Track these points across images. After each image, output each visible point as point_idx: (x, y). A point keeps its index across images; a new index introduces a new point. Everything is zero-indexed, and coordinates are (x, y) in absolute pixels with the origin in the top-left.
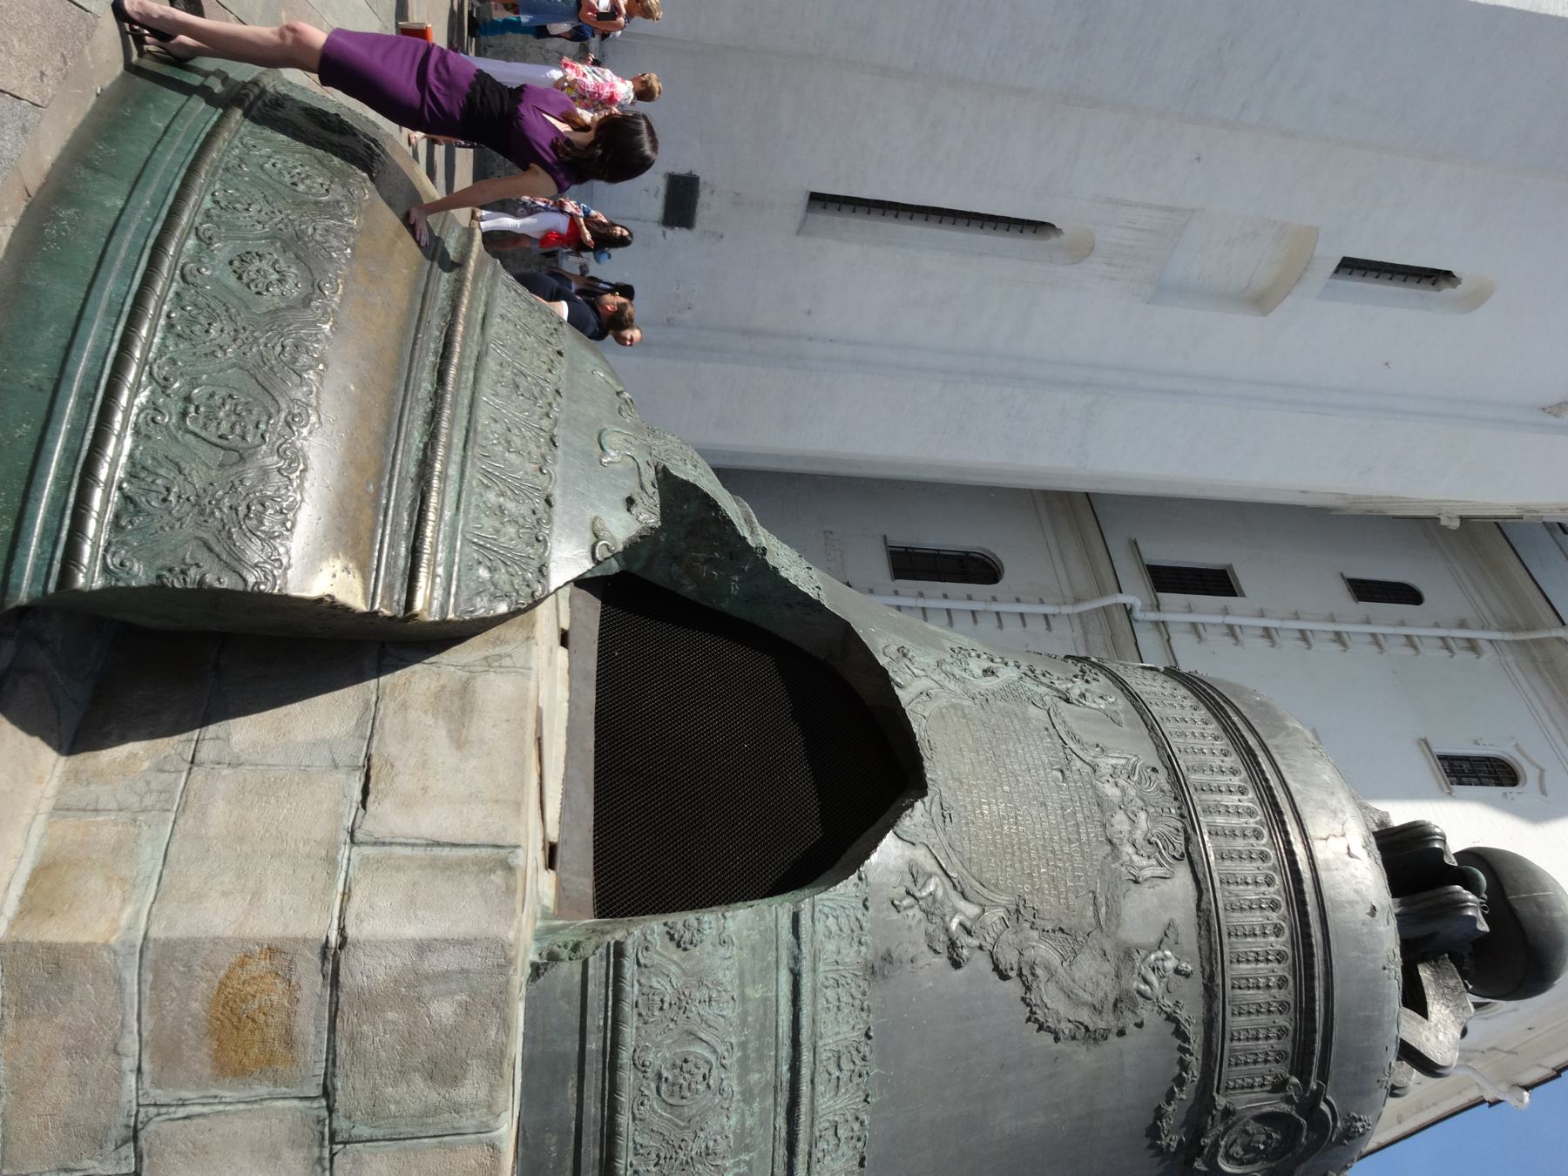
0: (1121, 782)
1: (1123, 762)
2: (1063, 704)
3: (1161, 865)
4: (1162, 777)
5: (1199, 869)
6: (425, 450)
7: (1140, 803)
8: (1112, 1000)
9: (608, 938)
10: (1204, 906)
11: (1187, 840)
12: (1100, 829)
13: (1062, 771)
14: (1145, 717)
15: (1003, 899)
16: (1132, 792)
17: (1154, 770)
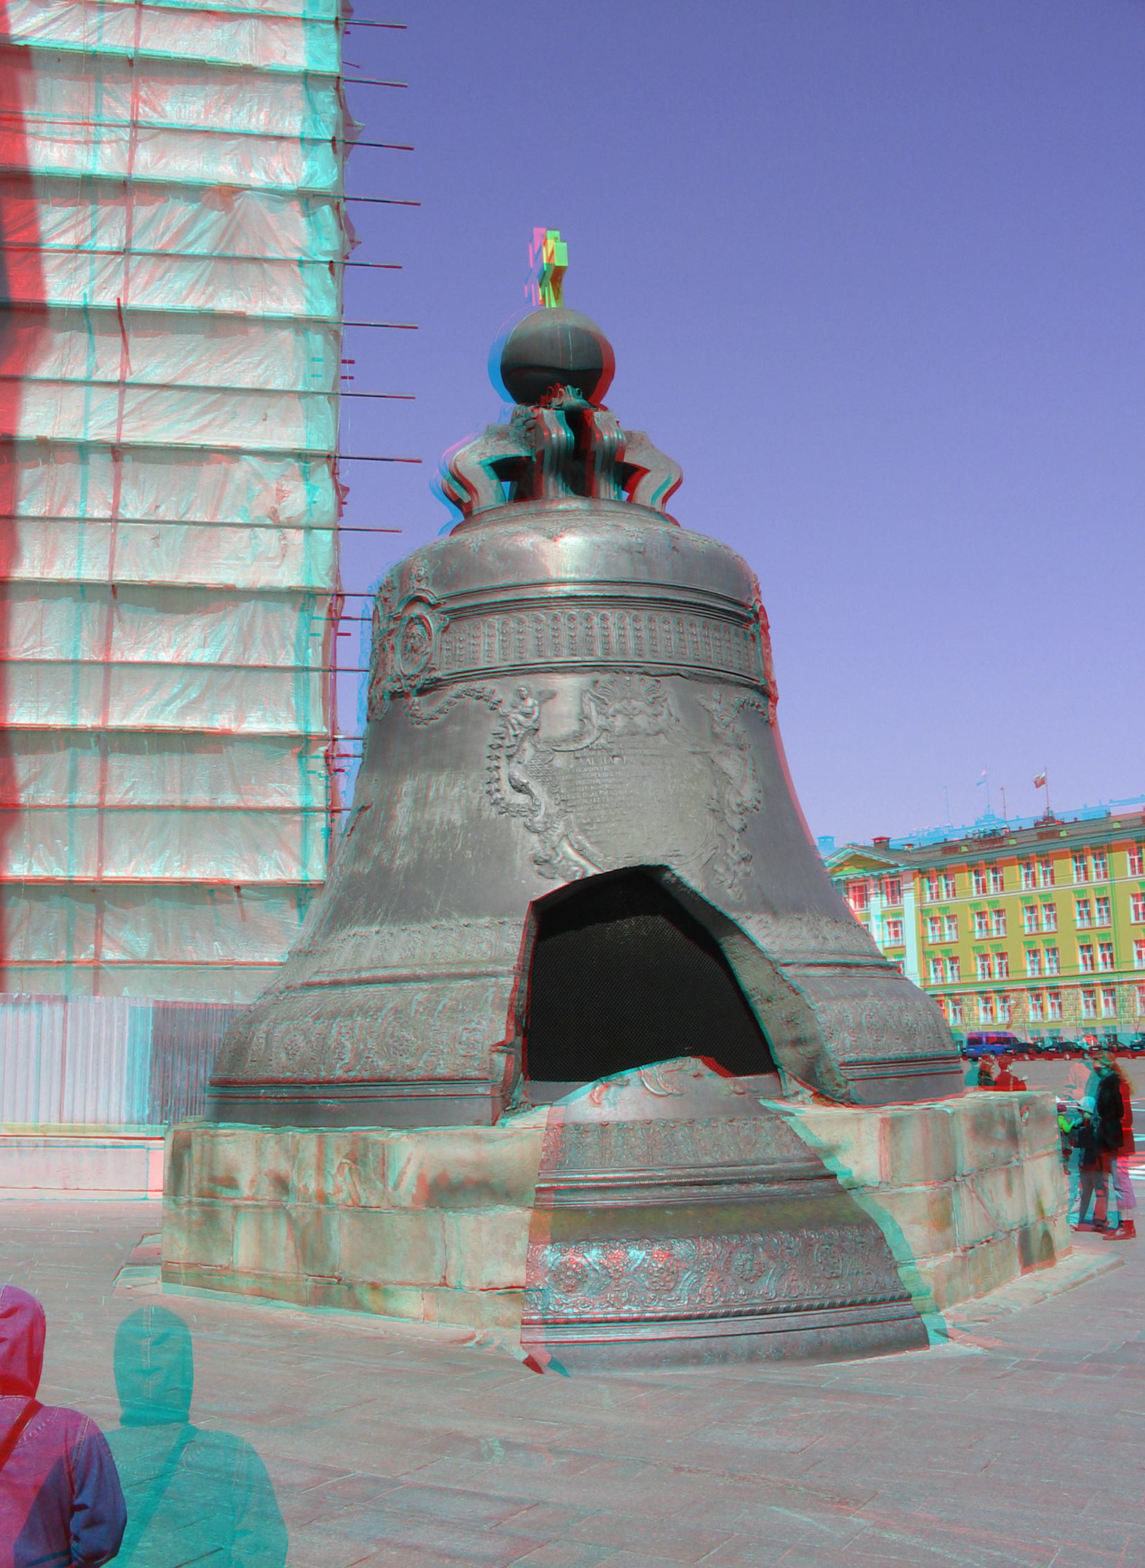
0: (611, 711)
1: (592, 705)
2: (541, 734)
3: (665, 700)
4: (604, 678)
5: (666, 672)
6: (763, 1183)
7: (625, 702)
8: (740, 753)
9: (837, 1070)
10: (686, 675)
11: (646, 674)
12: (651, 738)
13: (614, 757)
14: (543, 670)
15: (710, 819)
16: (618, 706)
17: (597, 682)
